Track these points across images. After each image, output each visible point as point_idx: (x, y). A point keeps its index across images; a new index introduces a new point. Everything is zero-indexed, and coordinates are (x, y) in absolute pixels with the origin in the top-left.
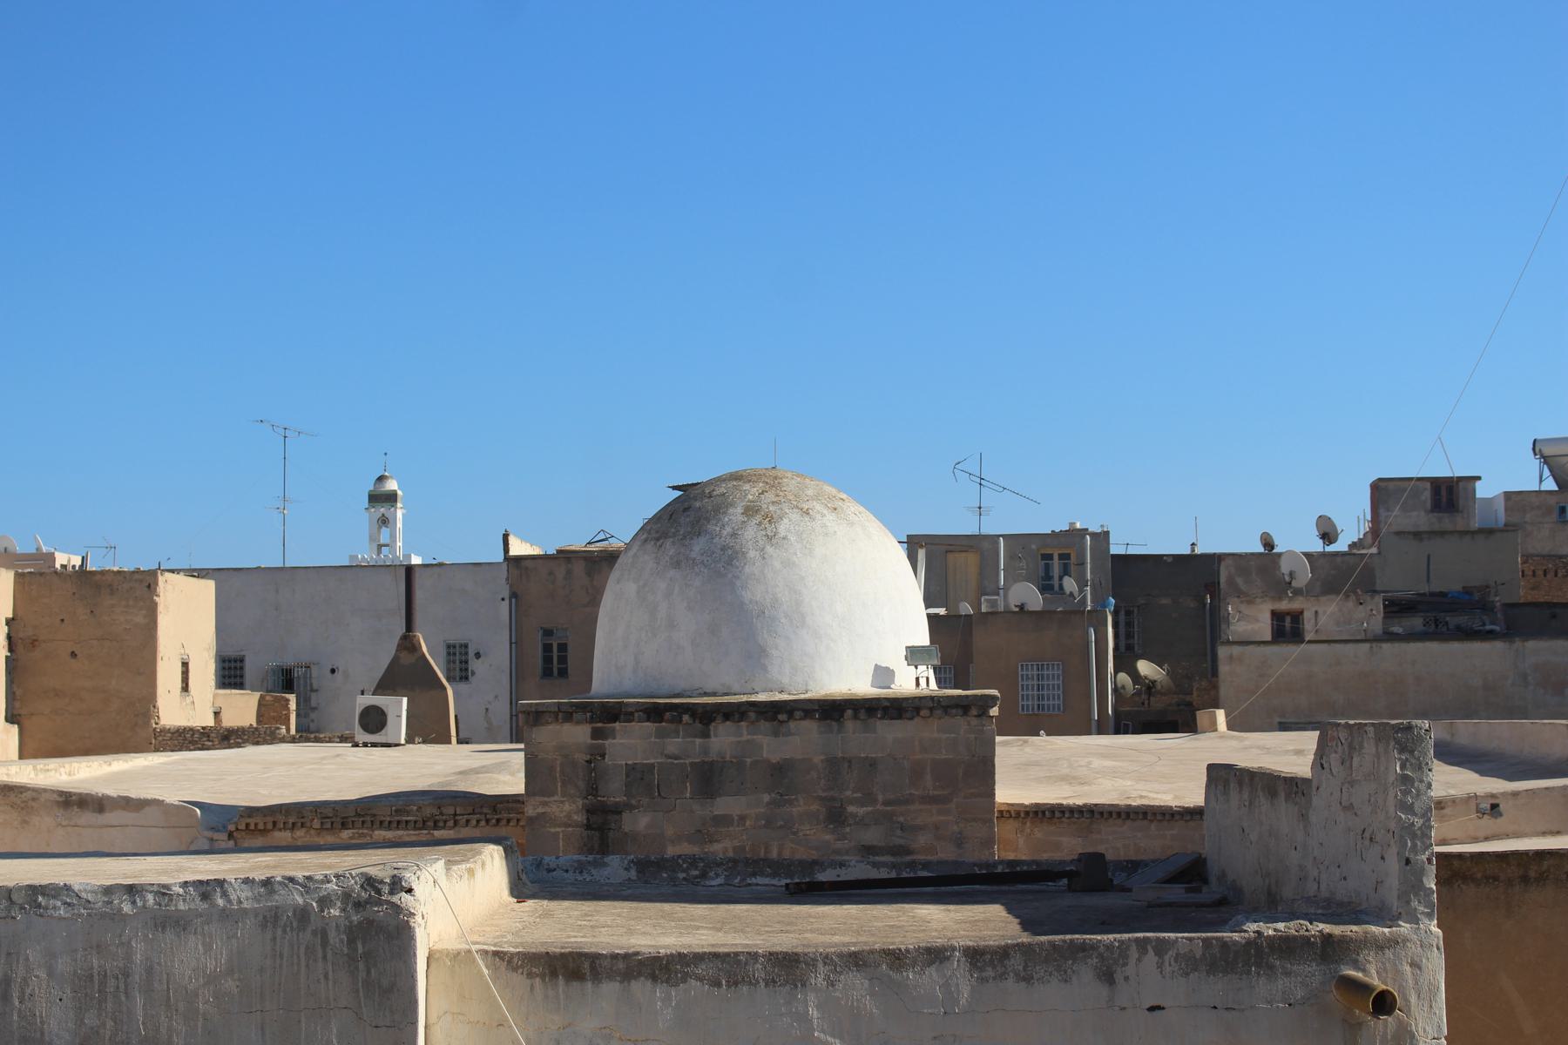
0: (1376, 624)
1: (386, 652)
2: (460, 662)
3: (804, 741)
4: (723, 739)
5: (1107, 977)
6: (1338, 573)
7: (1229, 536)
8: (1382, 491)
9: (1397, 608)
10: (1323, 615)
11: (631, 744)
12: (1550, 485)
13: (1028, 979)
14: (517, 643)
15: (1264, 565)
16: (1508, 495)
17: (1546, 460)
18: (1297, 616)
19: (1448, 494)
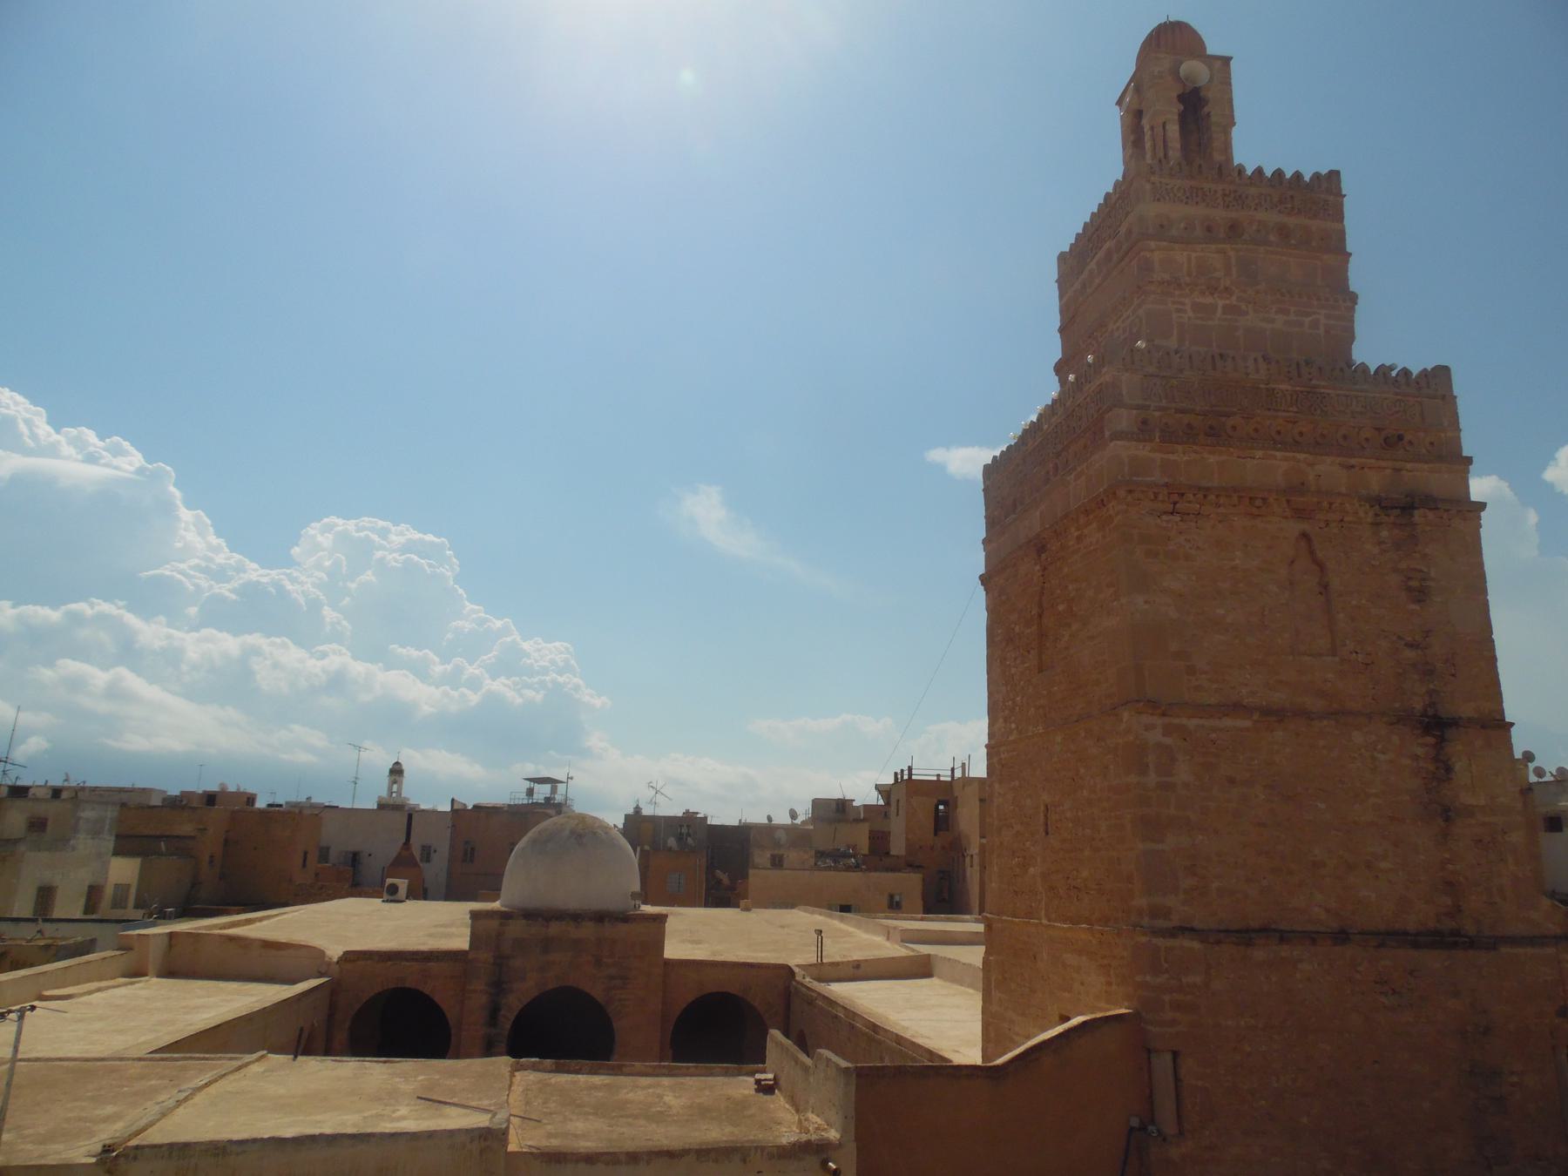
0: (812, 861)
1: (394, 850)
2: (427, 852)
3: (588, 930)
4: (555, 929)
5: (744, 1161)
6: (797, 836)
7: (757, 817)
8: (816, 803)
9: (821, 854)
10: (792, 856)
11: (516, 928)
12: (881, 802)
13: (716, 1161)
14: (452, 847)
15: (769, 830)
16: (865, 806)
17: (880, 792)
18: (781, 858)
19: (842, 806)
